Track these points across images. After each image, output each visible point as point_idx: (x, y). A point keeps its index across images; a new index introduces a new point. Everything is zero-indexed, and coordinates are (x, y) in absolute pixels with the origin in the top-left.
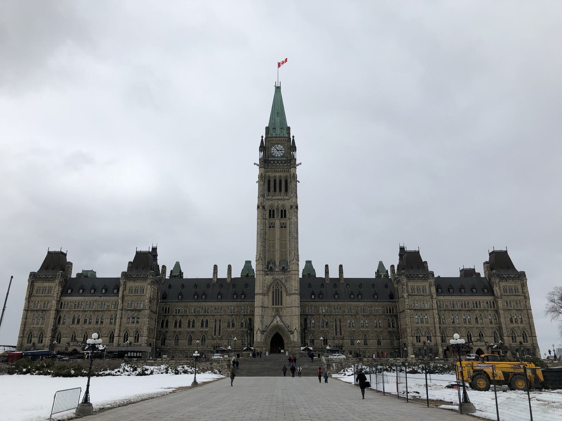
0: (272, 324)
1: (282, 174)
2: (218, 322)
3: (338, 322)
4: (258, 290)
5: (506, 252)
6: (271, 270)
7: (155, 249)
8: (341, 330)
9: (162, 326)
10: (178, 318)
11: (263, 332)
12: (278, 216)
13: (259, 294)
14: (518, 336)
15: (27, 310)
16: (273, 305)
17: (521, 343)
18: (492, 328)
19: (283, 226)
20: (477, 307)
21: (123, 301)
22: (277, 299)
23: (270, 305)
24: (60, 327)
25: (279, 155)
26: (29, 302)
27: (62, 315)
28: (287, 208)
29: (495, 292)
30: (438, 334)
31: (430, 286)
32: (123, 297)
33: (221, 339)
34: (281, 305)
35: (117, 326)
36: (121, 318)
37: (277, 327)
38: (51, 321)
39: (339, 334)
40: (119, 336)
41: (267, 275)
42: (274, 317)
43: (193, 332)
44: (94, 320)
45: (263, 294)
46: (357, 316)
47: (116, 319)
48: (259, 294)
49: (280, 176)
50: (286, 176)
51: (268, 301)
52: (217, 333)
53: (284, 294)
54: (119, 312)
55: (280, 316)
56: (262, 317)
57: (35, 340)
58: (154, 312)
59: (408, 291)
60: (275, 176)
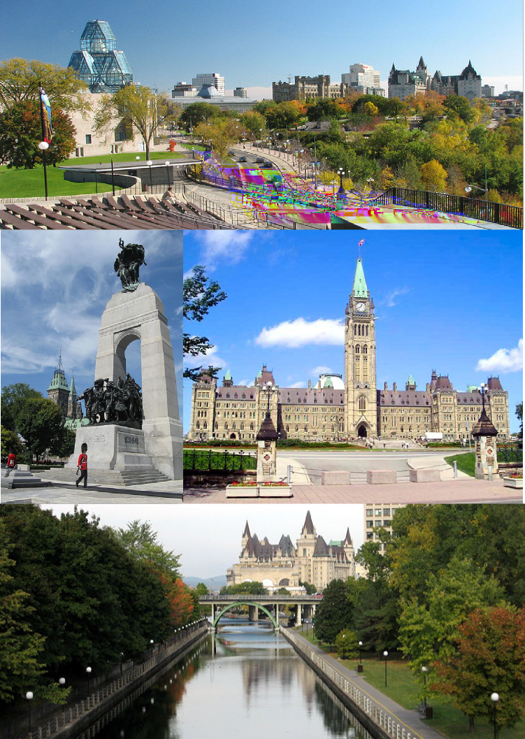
4: (351, 399)
10: (288, 415)
11: (354, 425)
19: (365, 359)
22: (362, 405)
23: (358, 409)
27: (217, 411)
33: (318, 428)
35: (256, 419)
37: (363, 422)
38: (212, 416)
40: (258, 426)
44: (239, 415)
45: (354, 402)
47: (254, 414)
51: (357, 406)
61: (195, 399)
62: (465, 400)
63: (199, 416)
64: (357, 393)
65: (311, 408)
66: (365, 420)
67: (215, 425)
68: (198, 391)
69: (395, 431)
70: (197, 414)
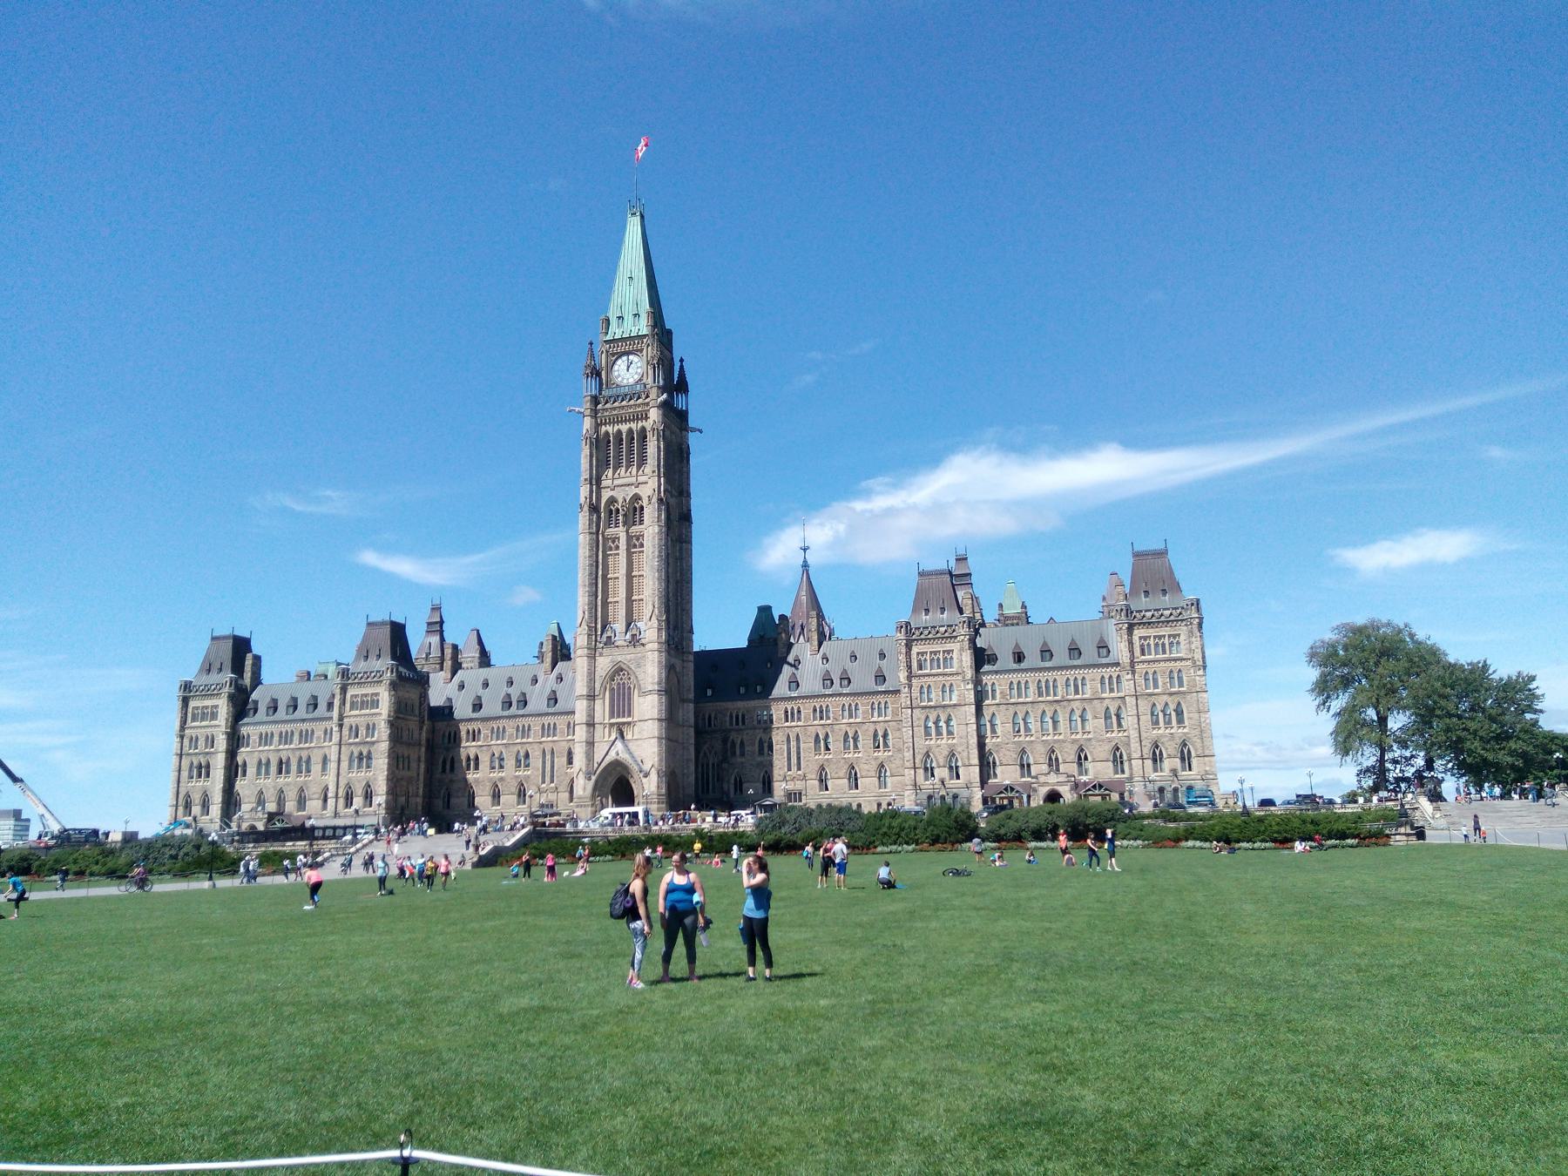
0: (608, 759)
1: (633, 425)
2: (548, 757)
3: (793, 743)
5: (1162, 554)
6: (609, 642)
7: (436, 609)
8: (799, 758)
9: (444, 771)
12: (625, 523)
14: (1169, 757)
15: (181, 756)
16: (612, 716)
17: (1174, 772)
18: (1110, 741)
19: (634, 543)
20: (1077, 692)
21: (341, 726)
22: (622, 703)
24: (241, 785)
25: (631, 381)
26: (182, 737)
27: (240, 759)
28: (645, 503)
30: (976, 761)
31: (962, 649)
32: (341, 718)
37: (617, 764)
38: (218, 774)
39: (794, 768)
40: (337, 797)
43: (502, 779)
44: (294, 767)
49: (630, 431)
50: (644, 429)
51: (602, 709)
52: (548, 779)
54: (335, 749)
56: (591, 744)
57: (196, 810)
58: (409, 745)
59: (909, 667)
60: (619, 432)
61: (182, 728)
62: (1019, 657)
64: (604, 664)
65: (536, 724)
66: (624, 756)
67: (231, 802)
68: (192, 704)
69: (799, 785)
70: (185, 774)
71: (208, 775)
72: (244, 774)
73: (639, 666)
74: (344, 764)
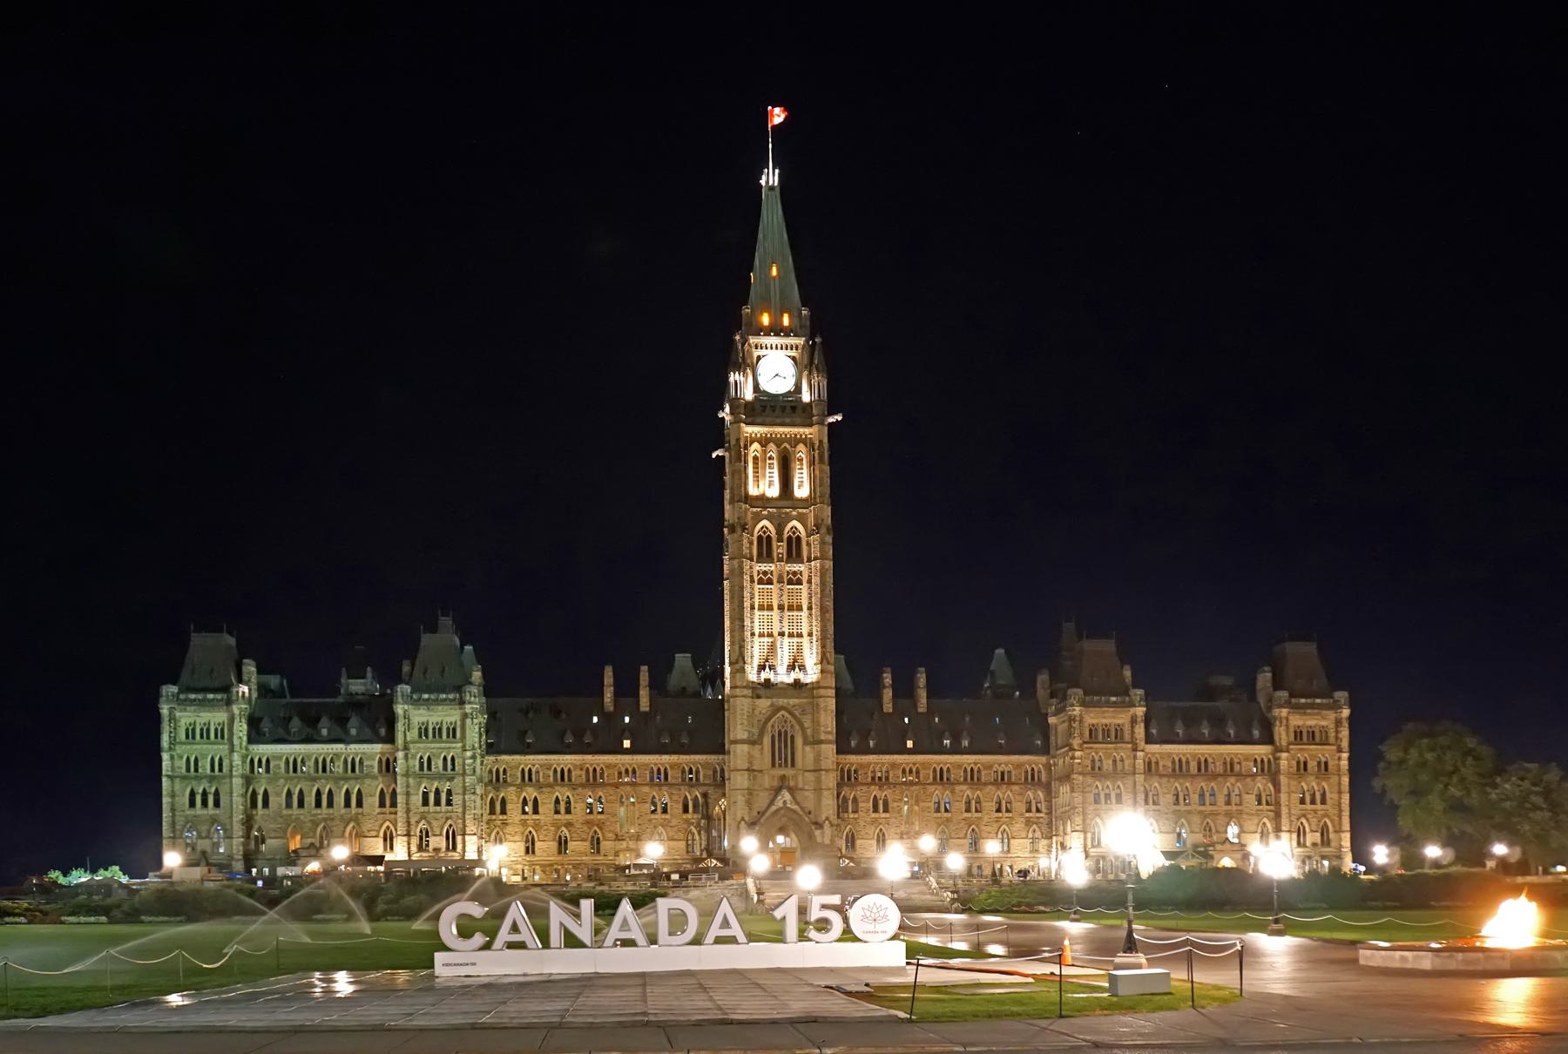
0: (774, 808)
13: (743, 742)
16: (773, 765)
29: (1276, 738)
31: (1133, 721)
34: (793, 765)
36: (408, 794)
38: (238, 801)
41: (759, 697)
42: (778, 791)
44: (340, 799)
45: (752, 742)
46: (958, 788)
48: (743, 742)
53: (799, 741)
55: (791, 790)
59: (1081, 734)
63: (192, 804)
71: (217, 804)
72: (266, 804)
73: (804, 713)
74: (417, 799)
